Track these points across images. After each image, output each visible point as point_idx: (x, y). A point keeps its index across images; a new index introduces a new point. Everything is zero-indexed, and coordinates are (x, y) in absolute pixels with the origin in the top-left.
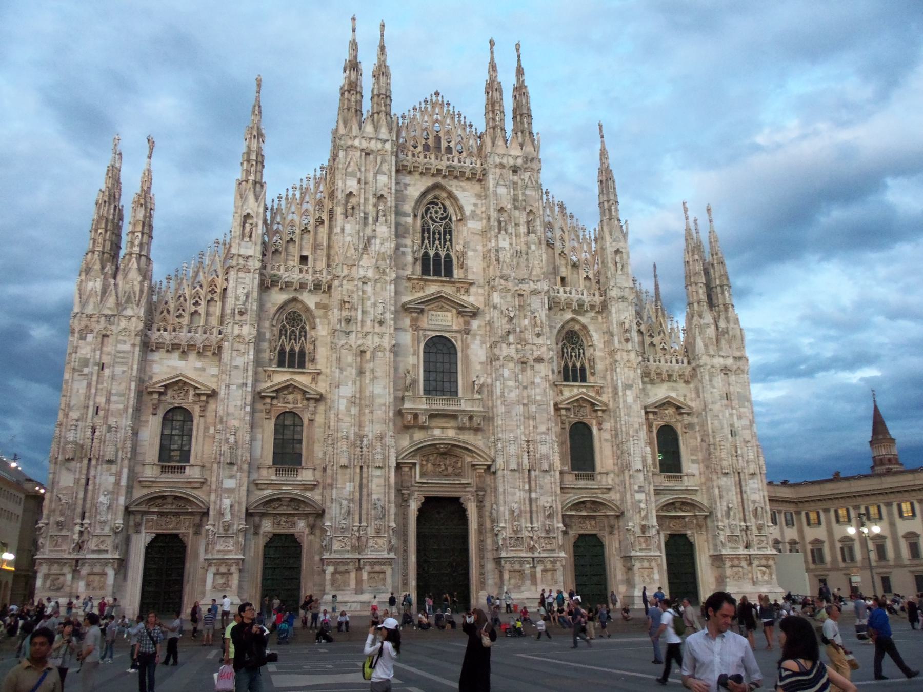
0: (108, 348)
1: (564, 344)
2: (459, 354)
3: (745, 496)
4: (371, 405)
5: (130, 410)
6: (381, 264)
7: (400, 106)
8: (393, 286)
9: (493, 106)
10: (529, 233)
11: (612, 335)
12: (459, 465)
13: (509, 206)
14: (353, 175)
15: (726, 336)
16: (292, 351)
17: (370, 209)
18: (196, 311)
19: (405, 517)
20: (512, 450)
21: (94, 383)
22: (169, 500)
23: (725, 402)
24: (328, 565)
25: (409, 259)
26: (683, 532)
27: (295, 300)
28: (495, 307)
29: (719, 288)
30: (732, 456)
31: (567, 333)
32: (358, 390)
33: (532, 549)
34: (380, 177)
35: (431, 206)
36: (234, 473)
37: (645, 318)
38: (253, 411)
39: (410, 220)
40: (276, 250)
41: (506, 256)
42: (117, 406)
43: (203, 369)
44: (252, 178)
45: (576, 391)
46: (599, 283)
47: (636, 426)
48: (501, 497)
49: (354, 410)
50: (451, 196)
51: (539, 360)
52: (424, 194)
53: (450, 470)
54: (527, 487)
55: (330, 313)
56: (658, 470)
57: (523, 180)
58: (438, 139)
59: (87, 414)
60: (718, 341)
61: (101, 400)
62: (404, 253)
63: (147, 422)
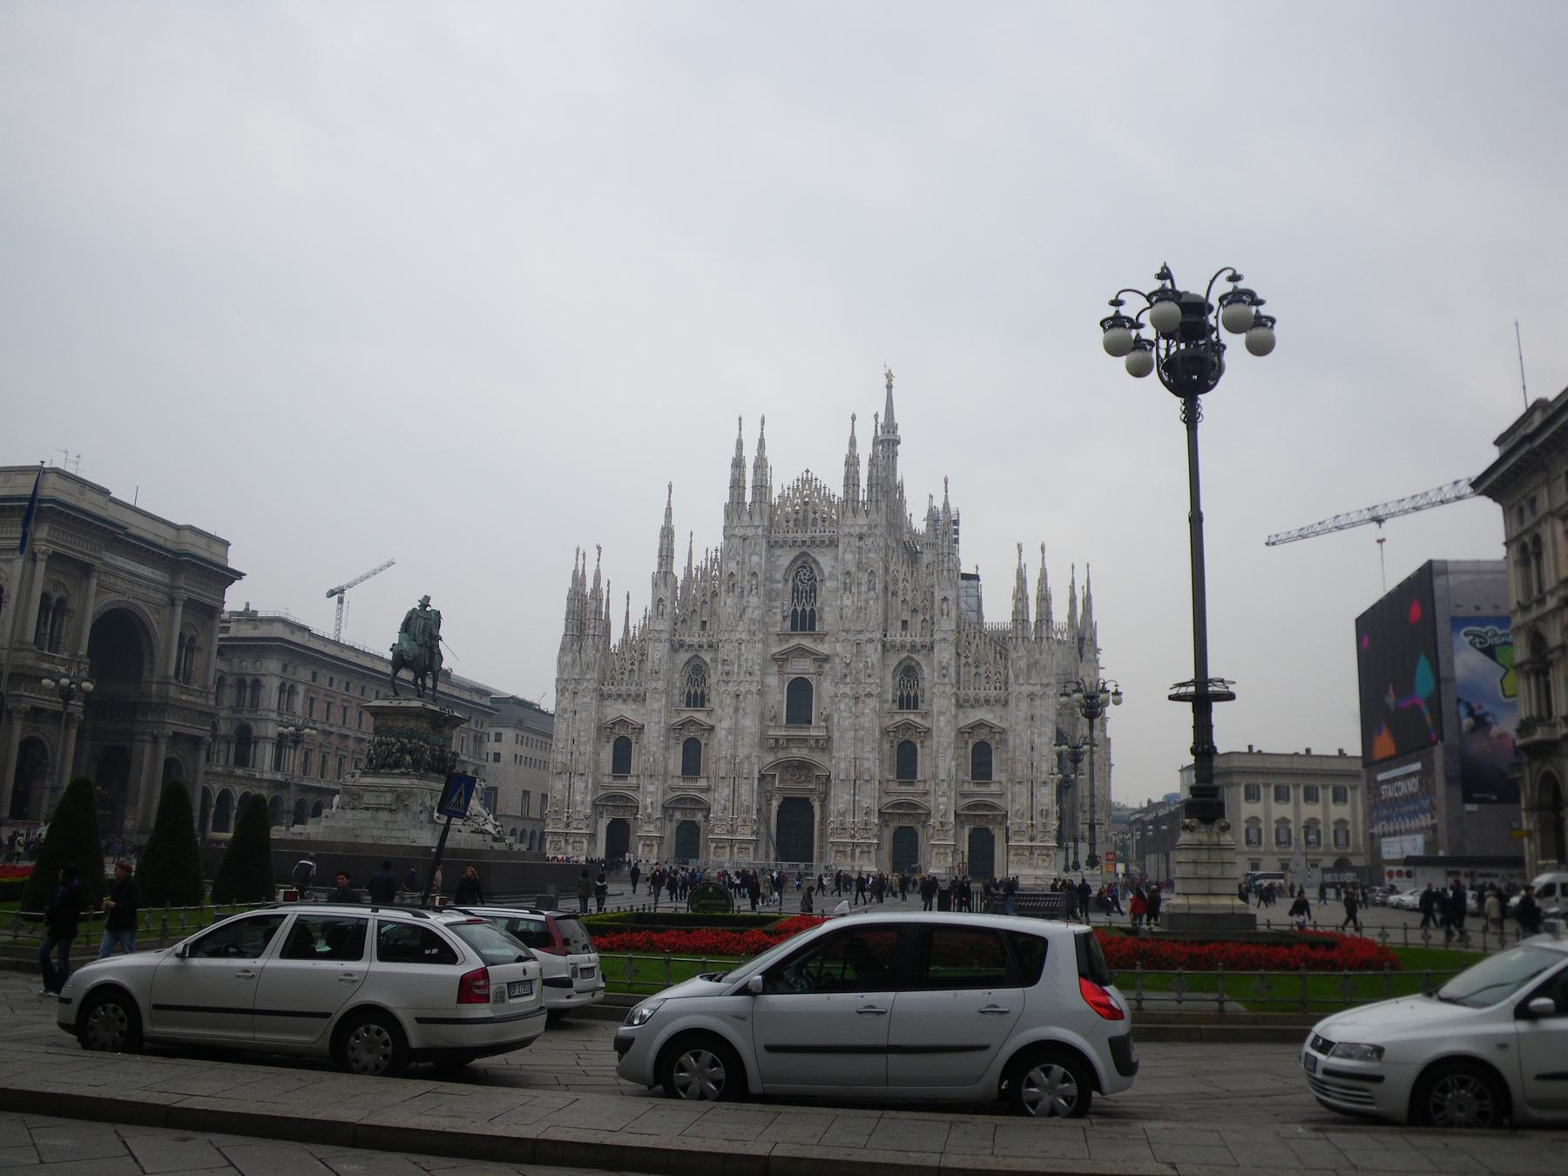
0: (578, 701)
6: (753, 628)
7: (776, 492)
9: (851, 481)
14: (733, 558)
19: (769, 811)
20: (842, 765)
25: (779, 617)
33: (853, 837)
38: (667, 738)
39: (780, 586)
41: (848, 612)
46: (929, 623)
51: (869, 695)
52: (794, 561)
58: (806, 511)
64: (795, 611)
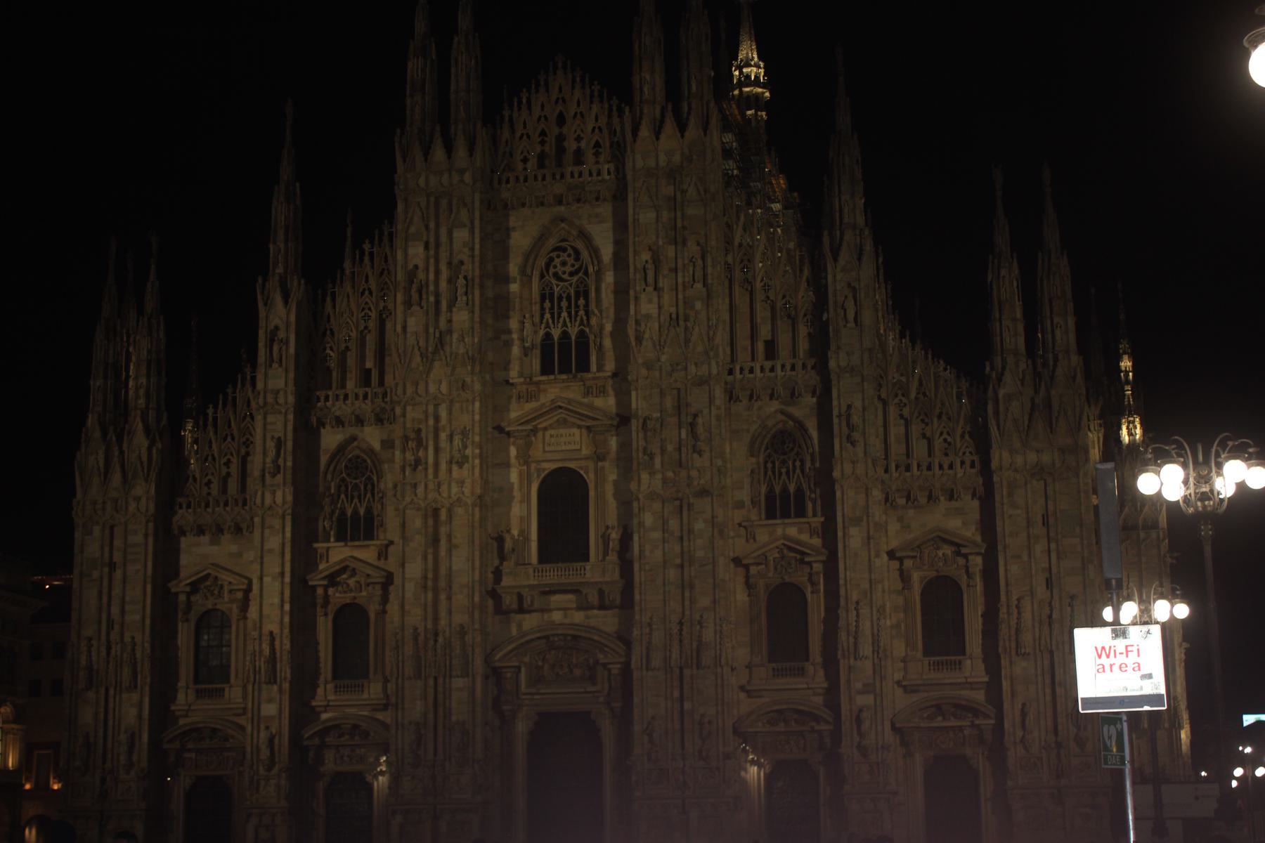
0: (118, 543)
1: (769, 456)
2: (592, 493)
3: (1058, 690)
4: (450, 588)
5: (148, 622)
8: (477, 404)
16: (356, 512)
17: (443, 285)
18: (228, 474)
21: (105, 590)
27: (354, 438)
30: (1041, 622)
34: (455, 234)
35: (554, 255)
37: (913, 395)
42: (133, 617)
43: (239, 555)
44: (280, 270)
50: (584, 235)
51: (703, 493)
52: (541, 239)
53: (578, 672)
54: (676, 694)
56: (919, 654)
57: (684, 192)
59: (100, 631)
60: (1030, 421)
61: (115, 610)
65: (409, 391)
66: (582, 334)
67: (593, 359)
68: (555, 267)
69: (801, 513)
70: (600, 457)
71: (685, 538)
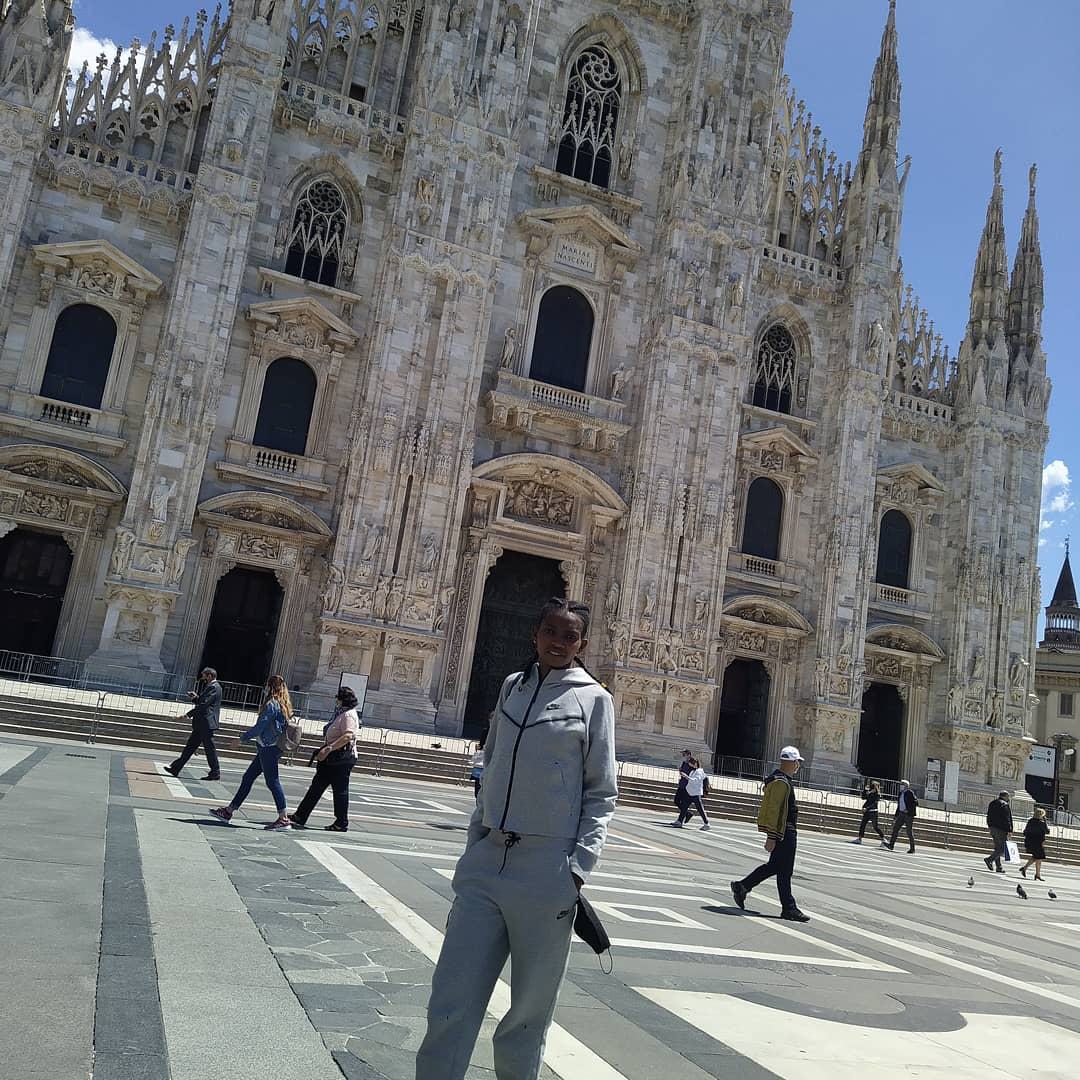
1: (764, 347)
2: (598, 325)
10: (750, 140)
11: (848, 346)
12: (568, 508)
13: (727, 84)
15: (1023, 384)
16: (315, 252)
18: (146, 136)
20: (663, 498)
22: (52, 471)
23: (1000, 490)
24: (328, 631)
25: (541, 138)
26: (893, 681)
28: (672, 255)
29: (1025, 305)
31: (771, 330)
32: (425, 342)
35: (590, 55)
36: (181, 442)
39: (553, 69)
40: (311, 61)
41: (705, 173)
45: (771, 424)
47: (860, 500)
48: (630, 573)
49: (414, 378)
51: (729, 361)
53: (552, 513)
54: (673, 564)
55: (392, 200)
57: (758, 43)
62: (533, 126)
63: (27, 317)
64: (568, 140)
65: (432, 127)
66: (604, 152)
67: (613, 182)
68: (589, 68)
69: (785, 409)
70: (614, 286)
71: (704, 402)
